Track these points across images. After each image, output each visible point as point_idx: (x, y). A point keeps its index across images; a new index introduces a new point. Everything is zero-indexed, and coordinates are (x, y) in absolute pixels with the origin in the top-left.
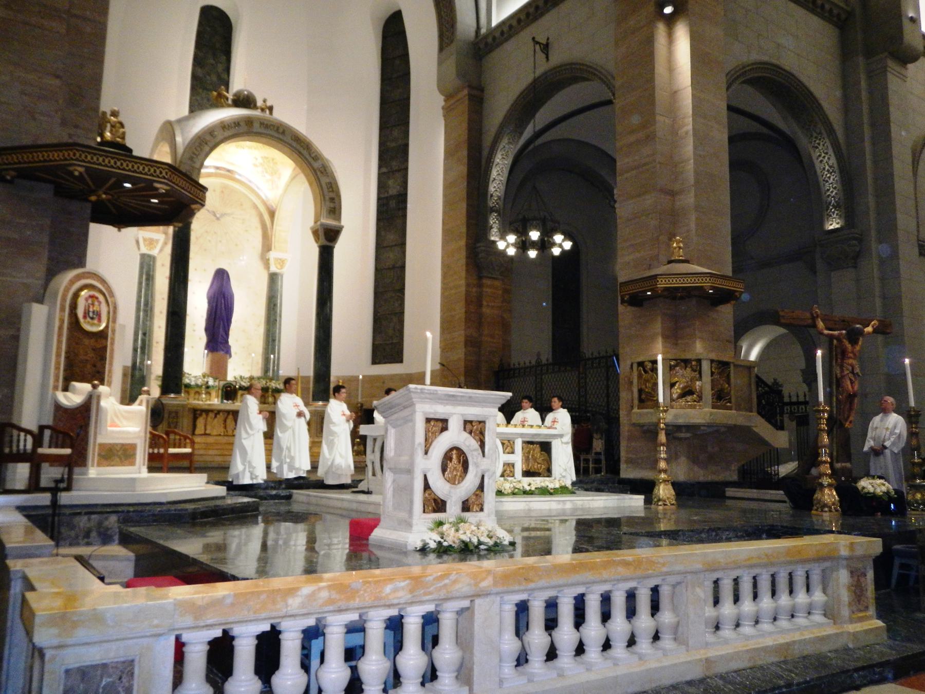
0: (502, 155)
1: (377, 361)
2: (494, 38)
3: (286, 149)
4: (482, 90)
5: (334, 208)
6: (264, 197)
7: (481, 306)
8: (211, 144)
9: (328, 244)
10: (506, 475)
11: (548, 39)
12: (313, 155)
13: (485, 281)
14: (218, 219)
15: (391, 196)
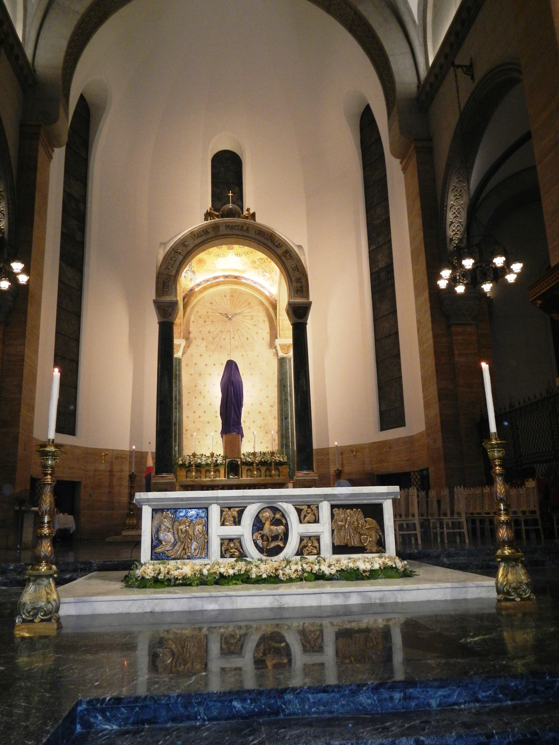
0: (454, 196)
1: (385, 427)
2: (431, 85)
3: (254, 244)
4: (430, 139)
5: (302, 287)
6: (268, 294)
7: (453, 355)
8: (184, 253)
9: (299, 321)
10: (305, 554)
11: (471, 59)
12: (277, 244)
13: (453, 329)
14: (230, 319)
15: (381, 269)
